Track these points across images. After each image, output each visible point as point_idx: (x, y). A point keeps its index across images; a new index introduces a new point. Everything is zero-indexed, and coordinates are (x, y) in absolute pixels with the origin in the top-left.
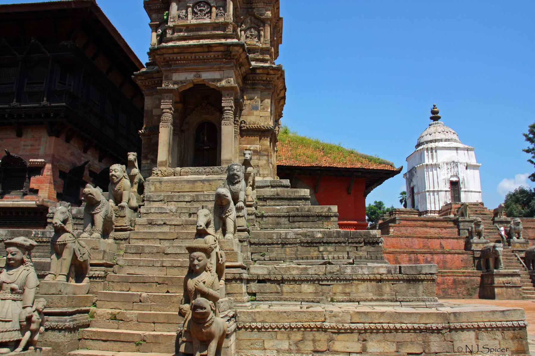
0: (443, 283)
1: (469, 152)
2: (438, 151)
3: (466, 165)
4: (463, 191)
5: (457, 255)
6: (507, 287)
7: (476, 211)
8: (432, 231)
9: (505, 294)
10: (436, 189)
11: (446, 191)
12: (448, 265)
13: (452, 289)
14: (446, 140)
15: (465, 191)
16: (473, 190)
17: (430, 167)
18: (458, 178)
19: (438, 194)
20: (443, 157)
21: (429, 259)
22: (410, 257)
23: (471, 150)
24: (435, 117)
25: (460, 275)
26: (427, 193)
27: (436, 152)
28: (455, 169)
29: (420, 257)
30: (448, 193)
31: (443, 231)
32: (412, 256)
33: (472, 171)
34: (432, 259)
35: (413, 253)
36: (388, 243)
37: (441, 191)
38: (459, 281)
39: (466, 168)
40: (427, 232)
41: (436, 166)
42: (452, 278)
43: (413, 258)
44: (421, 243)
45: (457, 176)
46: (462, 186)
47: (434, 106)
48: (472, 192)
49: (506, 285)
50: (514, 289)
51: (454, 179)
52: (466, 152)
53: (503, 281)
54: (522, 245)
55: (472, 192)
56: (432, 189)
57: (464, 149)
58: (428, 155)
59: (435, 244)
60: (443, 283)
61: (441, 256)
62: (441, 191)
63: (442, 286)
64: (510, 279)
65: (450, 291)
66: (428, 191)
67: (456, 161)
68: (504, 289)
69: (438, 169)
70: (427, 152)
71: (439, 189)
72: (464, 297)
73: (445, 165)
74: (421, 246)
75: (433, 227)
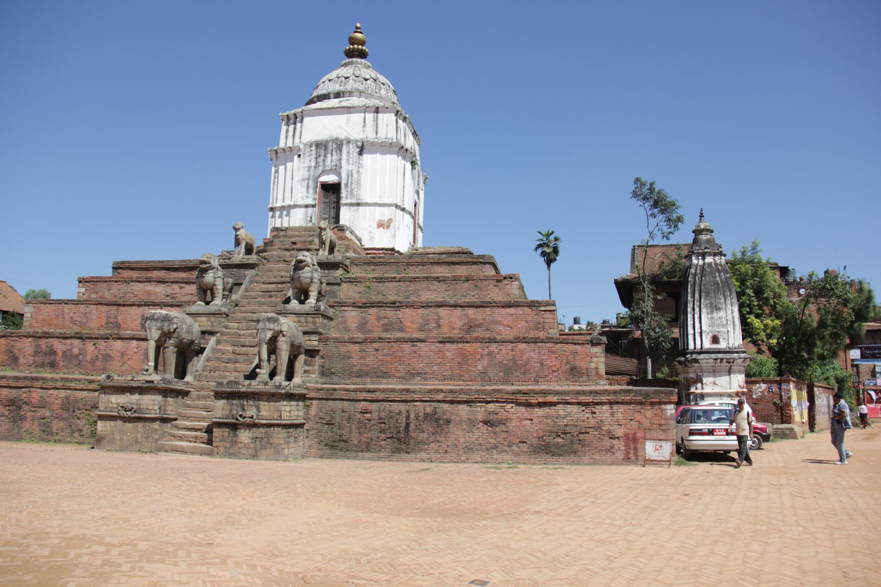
0: (43, 405)
1: (380, 115)
2: (305, 119)
3: (360, 144)
4: (346, 205)
5: (135, 343)
6: (126, 420)
7: (294, 243)
8: (159, 291)
9: (118, 437)
10: (288, 202)
11: (307, 206)
12: (115, 365)
13: (61, 419)
14: (338, 95)
15: (351, 205)
16: (369, 201)
17: (280, 155)
18: (339, 174)
19: (288, 215)
20: (317, 127)
21: (76, 351)
22: (37, 346)
23: (386, 110)
24: (356, 53)
25: (81, 386)
26: (271, 214)
27: (302, 122)
28: (335, 157)
29: (59, 346)
30: (310, 210)
31: (183, 291)
32: (43, 343)
33: (379, 157)
34: (83, 352)
35: (46, 336)
36: (40, 318)
37: (295, 206)
38: (77, 401)
39: (361, 153)
40: (149, 293)
41: (291, 152)
42: (63, 393)
43: (44, 347)
44: (104, 315)
45: (337, 170)
46: (344, 192)
47: (357, 28)
48: (366, 204)
49: (123, 413)
50: (140, 425)
51: (331, 178)
52: (370, 116)
53: (118, 404)
54: (303, 319)
55: (366, 204)
56: (279, 204)
57: (365, 109)
58: (287, 131)
59: (131, 318)
60: (43, 405)
61: (102, 344)
62: (295, 206)
63: (41, 412)
64: (135, 397)
65: (56, 425)
66: (272, 209)
67: (342, 137)
68: (119, 422)
69: (296, 157)
70: (288, 124)
71: (292, 203)
72: (81, 440)
73: (313, 148)
74: (104, 321)
75: (164, 282)
